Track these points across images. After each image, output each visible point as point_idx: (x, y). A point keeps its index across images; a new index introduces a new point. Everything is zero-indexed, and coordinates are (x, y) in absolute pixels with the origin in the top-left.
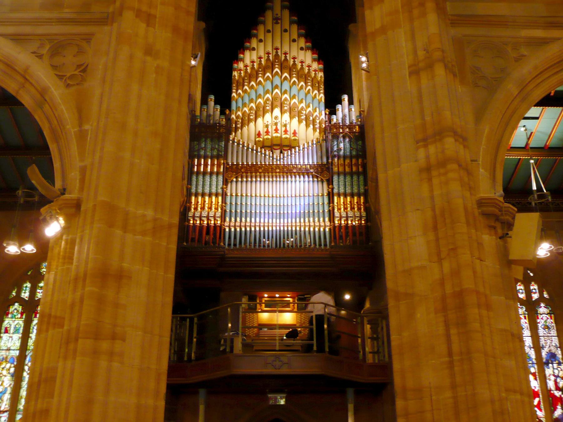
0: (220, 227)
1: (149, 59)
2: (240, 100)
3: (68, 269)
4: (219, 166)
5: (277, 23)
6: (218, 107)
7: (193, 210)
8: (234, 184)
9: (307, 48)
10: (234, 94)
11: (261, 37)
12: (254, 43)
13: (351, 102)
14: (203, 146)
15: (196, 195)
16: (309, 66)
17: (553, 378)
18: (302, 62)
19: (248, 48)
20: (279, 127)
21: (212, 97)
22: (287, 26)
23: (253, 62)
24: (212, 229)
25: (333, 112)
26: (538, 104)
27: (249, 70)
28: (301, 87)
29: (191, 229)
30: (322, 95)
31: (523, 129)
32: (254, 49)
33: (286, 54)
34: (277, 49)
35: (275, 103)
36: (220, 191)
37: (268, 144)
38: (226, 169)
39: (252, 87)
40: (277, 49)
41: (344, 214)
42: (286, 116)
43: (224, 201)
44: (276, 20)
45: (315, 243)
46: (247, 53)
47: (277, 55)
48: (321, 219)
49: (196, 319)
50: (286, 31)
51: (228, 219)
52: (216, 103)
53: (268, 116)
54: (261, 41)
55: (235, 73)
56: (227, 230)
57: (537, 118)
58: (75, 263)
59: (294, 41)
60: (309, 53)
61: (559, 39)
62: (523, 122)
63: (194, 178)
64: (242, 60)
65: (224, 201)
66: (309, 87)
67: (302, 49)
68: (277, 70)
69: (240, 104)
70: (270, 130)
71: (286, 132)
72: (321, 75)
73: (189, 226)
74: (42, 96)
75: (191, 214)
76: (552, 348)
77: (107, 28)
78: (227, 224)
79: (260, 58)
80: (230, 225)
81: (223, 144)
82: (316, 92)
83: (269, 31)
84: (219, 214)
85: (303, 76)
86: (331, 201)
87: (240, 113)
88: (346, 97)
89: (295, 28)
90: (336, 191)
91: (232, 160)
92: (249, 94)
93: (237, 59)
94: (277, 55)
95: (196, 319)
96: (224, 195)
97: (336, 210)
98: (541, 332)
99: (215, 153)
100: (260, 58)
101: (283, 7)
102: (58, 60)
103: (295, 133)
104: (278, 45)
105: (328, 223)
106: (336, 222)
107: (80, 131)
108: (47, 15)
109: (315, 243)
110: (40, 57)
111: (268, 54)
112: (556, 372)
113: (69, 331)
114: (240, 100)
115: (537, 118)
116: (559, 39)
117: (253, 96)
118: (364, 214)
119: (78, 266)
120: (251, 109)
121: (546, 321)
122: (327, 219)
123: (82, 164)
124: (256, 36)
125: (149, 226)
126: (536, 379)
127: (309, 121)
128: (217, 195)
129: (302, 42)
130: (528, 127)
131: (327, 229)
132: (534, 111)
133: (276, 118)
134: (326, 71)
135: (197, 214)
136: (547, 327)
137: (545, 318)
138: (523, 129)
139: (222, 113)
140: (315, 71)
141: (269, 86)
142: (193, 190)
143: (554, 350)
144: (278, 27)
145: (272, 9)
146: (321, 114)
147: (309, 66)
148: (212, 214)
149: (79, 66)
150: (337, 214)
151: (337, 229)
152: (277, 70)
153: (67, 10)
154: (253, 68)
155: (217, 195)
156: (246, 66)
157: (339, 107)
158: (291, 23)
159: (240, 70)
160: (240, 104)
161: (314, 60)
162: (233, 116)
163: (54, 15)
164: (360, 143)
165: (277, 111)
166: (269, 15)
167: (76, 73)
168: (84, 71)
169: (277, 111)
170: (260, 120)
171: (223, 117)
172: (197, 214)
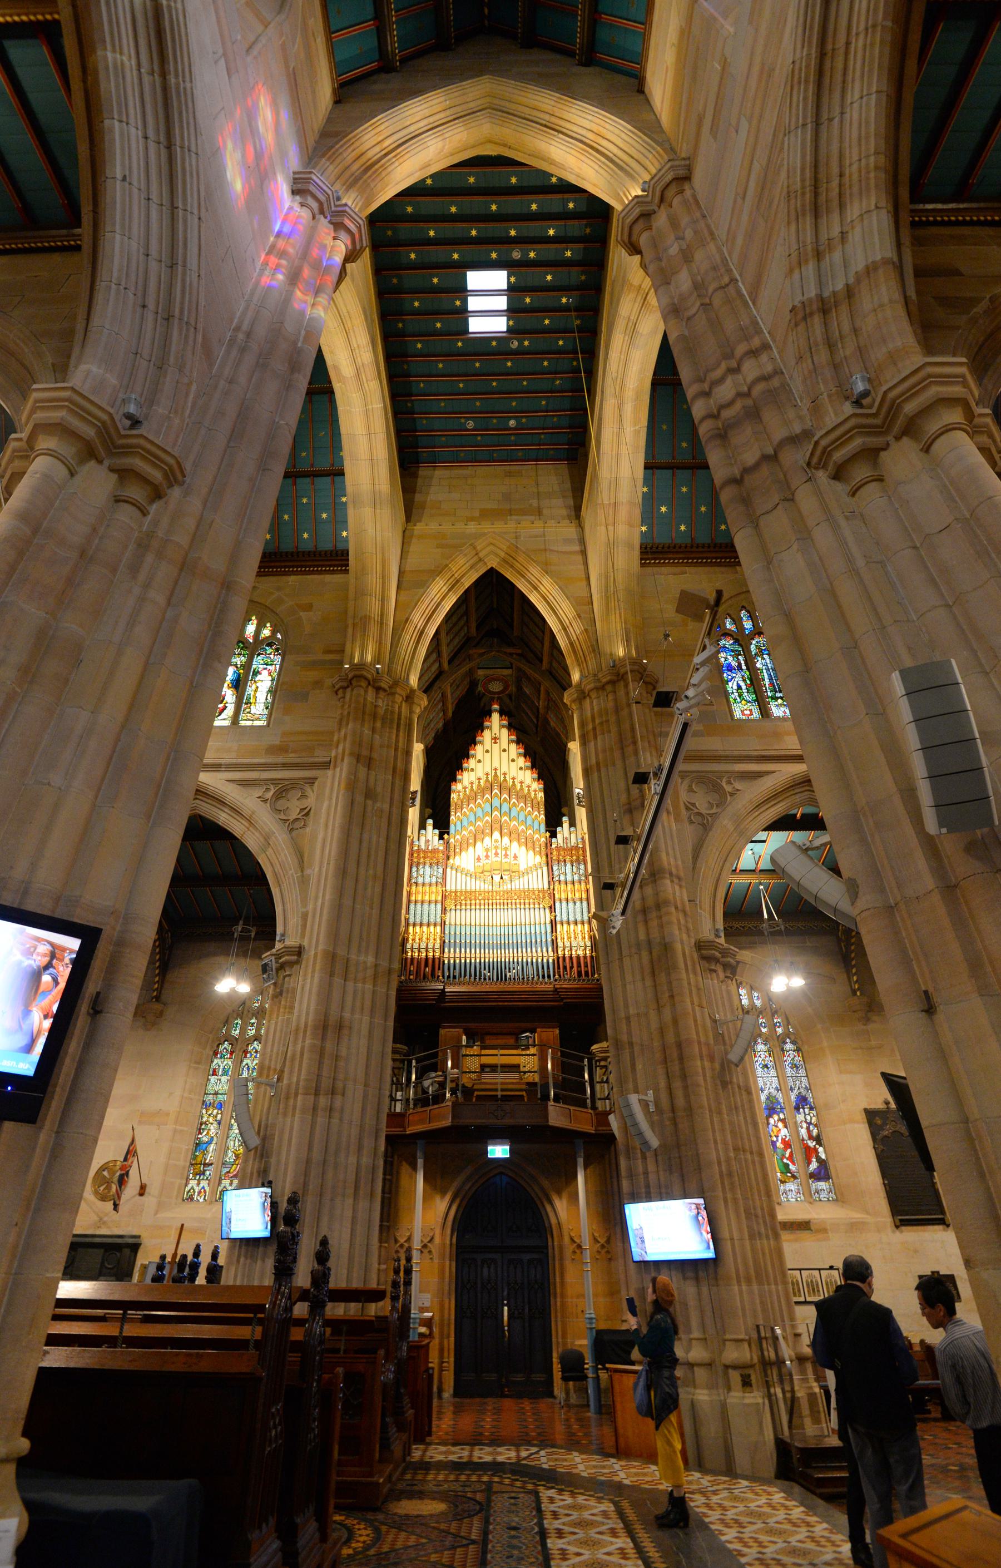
0: (439, 959)
1: (369, 802)
2: (459, 824)
3: (288, 1019)
4: (437, 893)
5: (495, 743)
6: (437, 831)
7: (410, 941)
8: (453, 912)
9: (527, 768)
10: (452, 817)
11: (479, 756)
12: (472, 763)
13: (572, 824)
14: (421, 872)
15: (414, 925)
16: (529, 787)
17: (805, 1125)
18: (521, 783)
19: (466, 769)
20: (499, 851)
21: (430, 821)
22: (505, 745)
23: (472, 783)
24: (430, 962)
25: (554, 835)
26: (765, 830)
27: (468, 792)
28: (522, 809)
29: (409, 961)
30: (543, 816)
31: (750, 852)
32: (472, 770)
33: (505, 774)
34: (496, 769)
35: (494, 826)
36: (439, 920)
37: (488, 868)
38: (444, 897)
39: (471, 810)
40: (496, 769)
41: (567, 944)
42: (506, 840)
43: (443, 931)
44: (495, 740)
45: (538, 975)
46: (465, 774)
47: (496, 775)
48: (544, 949)
49: (414, 1063)
50: (504, 750)
51: (446, 950)
52: (434, 828)
53: (487, 839)
54: (479, 761)
55: (453, 795)
56: (446, 962)
57: (764, 841)
58: (296, 1014)
59: (513, 760)
60: (528, 773)
61: (774, 772)
62: (750, 846)
63: (412, 906)
64: (461, 781)
65: (443, 931)
66: (529, 809)
67: (521, 769)
68: (496, 791)
69: (459, 827)
70: (489, 854)
71: (506, 855)
72: (541, 795)
73: (406, 959)
74: (266, 840)
75: (409, 946)
76: (802, 1090)
77: (330, 773)
78: (446, 955)
79: (479, 779)
80: (450, 956)
81: (441, 870)
82: (536, 813)
83: (487, 751)
84: (437, 946)
85: (524, 798)
86: (554, 929)
87: (458, 837)
88: (565, 819)
89: (513, 746)
90: (558, 919)
91: (450, 886)
92: (468, 817)
93: (454, 780)
94: (496, 775)
95: (414, 1063)
96: (443, 924)
97: (559, 940)
98: (789, 1071)
99: (434, 880)
100: (479, 779)
101: (502, 726)
102: (281, 804)
103: (515, 857)
104: (496, 764)
105: (551, 954)
106: (560, 953)
107: (303, 876)
108: (271, 760)
109: (538, 975)
110: (265, 801)
111: (487, 774)
112: (808, 1118)
113: (289, 1086)
114: (459, 824)
115: (764, 841)
116: (774, 772)
117: (472, 818)
118: (589, 944)
119: (299, 1016)
120: (470, 832)
121: (793, 1059)
122: (550, 949)
123: (304, 910)
124: (473, 756)
125: (370, 972)
126: (786, 1127)
127: (529, 843)
128: (435, 925)
129: (521, 761)
130: (755, 850)
131: (551, 961)
132: (762, 835)
133: (496, 841)
134: (546, 791)
135: (416, 946)
136: (794, 1066)
137: (792, 1056)
138: (750, 852)
139: (441, 837)
140: (535, 791)
141: (487, 808)
142: (411, 920)
143: (804, 1092)
144: (496, 747)
145: (490, 728)
146: (541, 836)
147: (529, 787)
148: (430, 945)
149: (302, 810)
150: (560, 944)
151: (561, 960)
152: (496, 791)
153: (291, 755)
154: (472, 789)
155: (435, 925)
156: (465, 788)
157: (559, 829)
158: (511, 741)
159: (459, 792)
160: (459, 827)
161: (534, 780)
162: (452, 840)
163: (281, 760)
164: (582, 867)
165: (496, 835)
166: (487, 733)
167: (299, 816)
168: (307, 814)
169: (496, 835)
170: (479, 844)
171: (441, 842)
172: (416, 946)
